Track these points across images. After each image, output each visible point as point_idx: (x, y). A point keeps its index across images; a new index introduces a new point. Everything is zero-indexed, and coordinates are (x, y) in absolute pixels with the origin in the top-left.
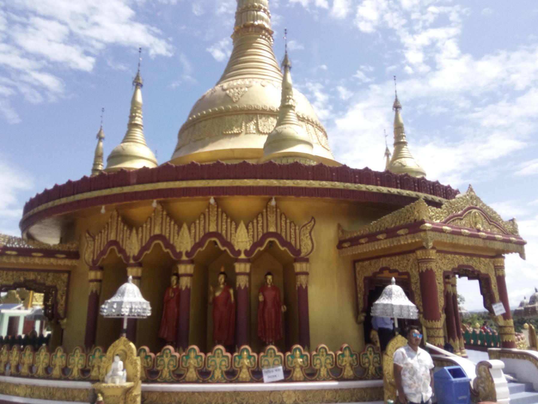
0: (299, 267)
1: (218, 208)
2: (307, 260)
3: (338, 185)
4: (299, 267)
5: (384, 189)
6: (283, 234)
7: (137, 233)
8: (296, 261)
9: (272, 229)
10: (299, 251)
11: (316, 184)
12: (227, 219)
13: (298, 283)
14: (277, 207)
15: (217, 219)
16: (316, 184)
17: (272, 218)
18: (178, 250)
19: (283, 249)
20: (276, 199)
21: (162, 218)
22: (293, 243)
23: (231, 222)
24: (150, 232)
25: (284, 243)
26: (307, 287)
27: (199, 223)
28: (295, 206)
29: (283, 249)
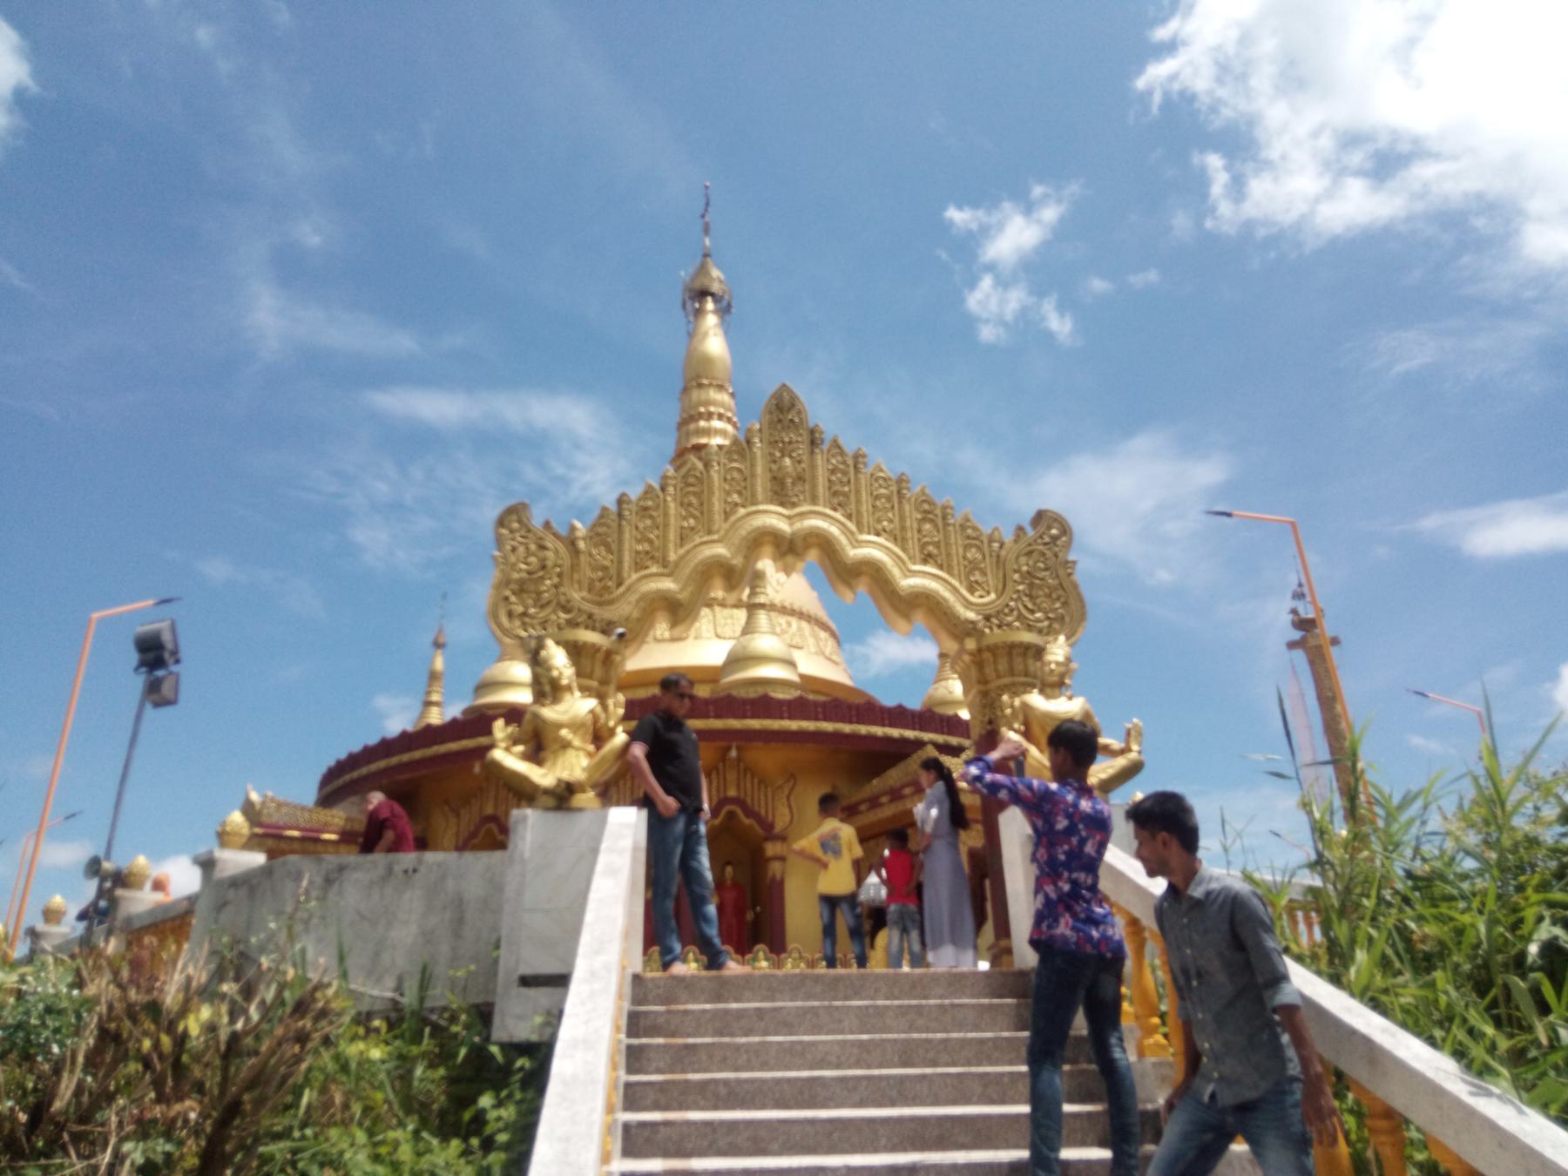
0: (771, 849)
2: (783, 838)
3: (828, 726)
4: (771, 849)
5: (895, 733)
6: (749, 801)
8: (766, 839)
9: (732, 793)
10: (771, 826)
11: (794, 725)
13: (770, 874)
14: (739, 759)
16: (794, 725)
17: (731, 776)
19: (747, 821)
20: (739, 749)
22: (763, 812)
25: (750, 813)
26: (782, 882)
28: (767, 759)
29: (747, 821)
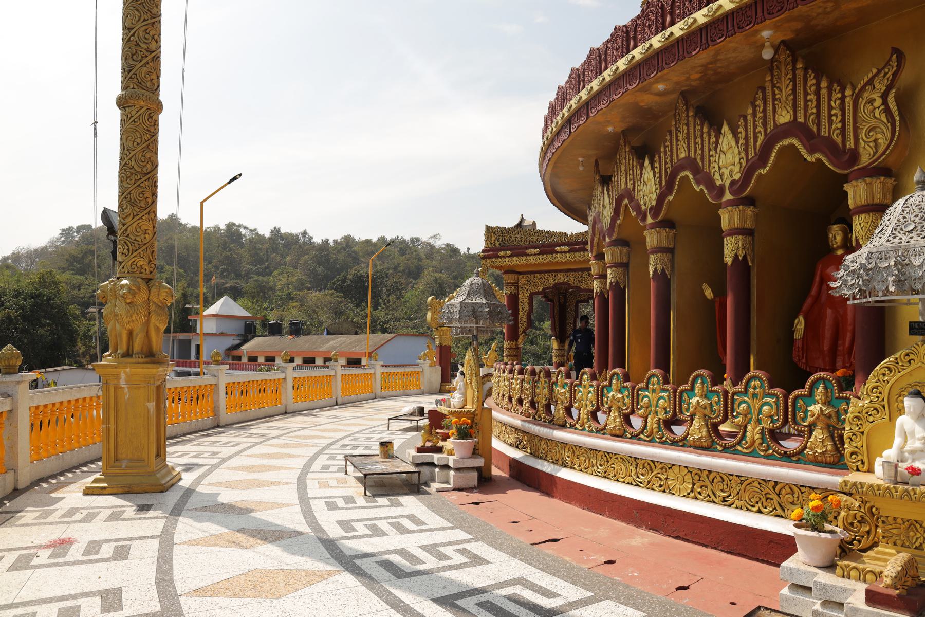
1: (794, 63)
7: (653, 168)
12: (818, 85)
15: (794, 91)
18: (718, 183)
21: (687, 125)
23: (830, 89)
24: (671, 161)
27: (754, 114)
